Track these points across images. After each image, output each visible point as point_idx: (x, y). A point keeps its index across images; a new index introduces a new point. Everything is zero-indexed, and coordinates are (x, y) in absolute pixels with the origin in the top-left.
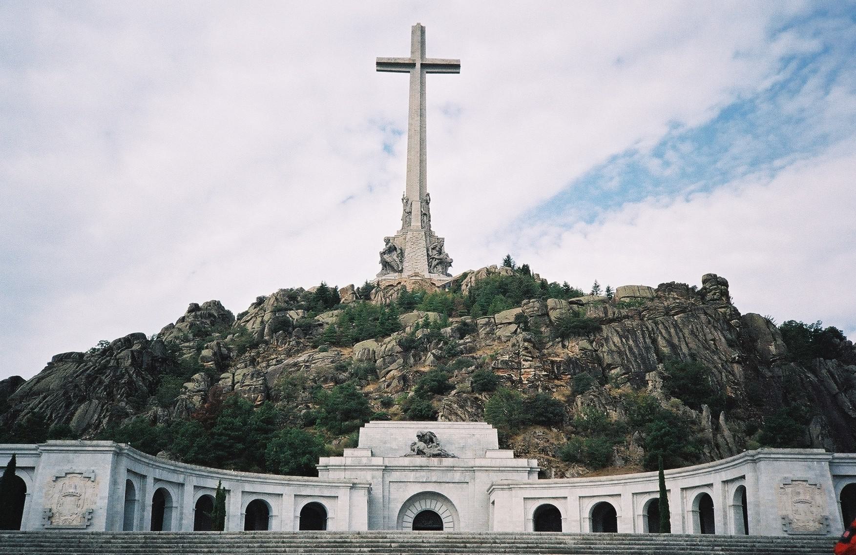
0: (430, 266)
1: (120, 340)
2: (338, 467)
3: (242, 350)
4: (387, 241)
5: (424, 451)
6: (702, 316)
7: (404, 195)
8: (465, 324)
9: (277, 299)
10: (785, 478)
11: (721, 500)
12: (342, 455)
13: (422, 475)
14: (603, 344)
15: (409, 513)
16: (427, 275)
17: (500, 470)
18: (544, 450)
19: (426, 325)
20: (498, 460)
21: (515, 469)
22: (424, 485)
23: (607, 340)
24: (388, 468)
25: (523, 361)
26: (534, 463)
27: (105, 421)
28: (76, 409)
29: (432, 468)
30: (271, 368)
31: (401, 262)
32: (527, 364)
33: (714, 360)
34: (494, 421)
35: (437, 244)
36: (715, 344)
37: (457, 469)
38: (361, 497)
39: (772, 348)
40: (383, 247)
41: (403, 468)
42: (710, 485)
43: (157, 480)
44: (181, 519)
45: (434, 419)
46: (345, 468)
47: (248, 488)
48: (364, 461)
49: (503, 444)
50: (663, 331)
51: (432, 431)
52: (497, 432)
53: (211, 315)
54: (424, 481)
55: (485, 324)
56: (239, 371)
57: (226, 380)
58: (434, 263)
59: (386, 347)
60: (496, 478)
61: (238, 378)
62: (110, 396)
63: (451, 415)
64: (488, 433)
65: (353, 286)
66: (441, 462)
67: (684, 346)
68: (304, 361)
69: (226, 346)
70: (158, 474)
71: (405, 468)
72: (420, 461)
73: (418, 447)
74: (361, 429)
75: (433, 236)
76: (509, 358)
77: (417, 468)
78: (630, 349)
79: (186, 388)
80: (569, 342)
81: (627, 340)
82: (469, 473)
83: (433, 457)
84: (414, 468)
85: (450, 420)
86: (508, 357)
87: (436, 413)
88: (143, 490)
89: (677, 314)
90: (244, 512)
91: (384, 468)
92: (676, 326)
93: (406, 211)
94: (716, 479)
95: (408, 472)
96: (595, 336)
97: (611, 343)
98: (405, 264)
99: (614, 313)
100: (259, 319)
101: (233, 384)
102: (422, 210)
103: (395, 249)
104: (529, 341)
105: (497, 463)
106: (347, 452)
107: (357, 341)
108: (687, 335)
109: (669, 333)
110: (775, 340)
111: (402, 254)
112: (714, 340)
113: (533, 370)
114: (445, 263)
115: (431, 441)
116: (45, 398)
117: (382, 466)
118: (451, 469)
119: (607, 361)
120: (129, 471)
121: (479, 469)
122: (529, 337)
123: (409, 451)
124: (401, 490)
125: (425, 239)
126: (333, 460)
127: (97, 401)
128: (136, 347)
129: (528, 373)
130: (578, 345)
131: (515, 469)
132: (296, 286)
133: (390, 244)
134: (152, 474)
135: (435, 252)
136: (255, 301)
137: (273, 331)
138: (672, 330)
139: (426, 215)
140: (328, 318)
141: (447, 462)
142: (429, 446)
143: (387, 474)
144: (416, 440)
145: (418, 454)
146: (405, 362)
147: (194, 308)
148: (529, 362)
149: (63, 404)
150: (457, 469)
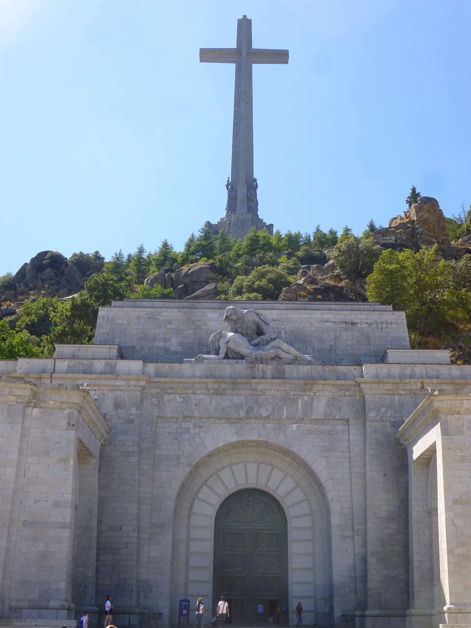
7: (228, 181)
73: (228, 342)
76: (396, 241)
91: (143, 383)
95: (202, 396)
102: (249, 195)
124: (187, 437)
145: (226, 357)
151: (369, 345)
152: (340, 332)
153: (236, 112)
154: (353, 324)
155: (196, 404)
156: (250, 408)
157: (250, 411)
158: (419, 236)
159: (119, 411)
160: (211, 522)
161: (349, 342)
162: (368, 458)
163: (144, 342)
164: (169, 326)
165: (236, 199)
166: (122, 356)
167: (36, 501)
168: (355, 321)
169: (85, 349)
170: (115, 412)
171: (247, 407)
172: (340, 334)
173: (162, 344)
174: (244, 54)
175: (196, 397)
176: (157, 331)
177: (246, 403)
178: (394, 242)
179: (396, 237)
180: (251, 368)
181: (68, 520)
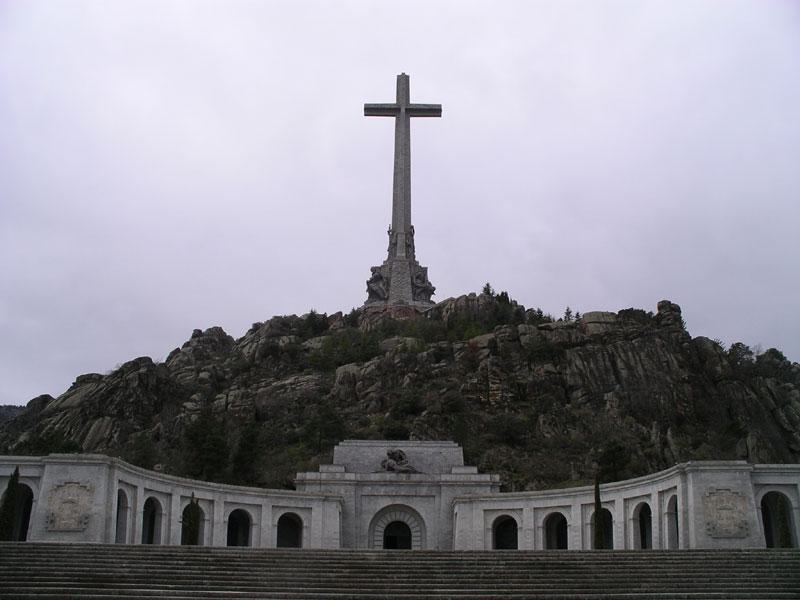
0: (414, 293)
1: (129, 363)
2: (313, 482)
3: (236, 373)
4: (374, 270)
6: (657, 340)
8: (441, 349)
9: (271, 326)
10: (711, 488)
11: (657, 509)
12: (318, 471)
13: (391, 490)
15: (380, 523)
16: (411, 303)
17: (464, 485)
18: (506, 467)
19: (405, 349)
21: (479, 484)
23: (570, 363)
26: (497, 477)
27: (116, 436)
28: (91, 425)
30: (260, 390)
31: (388, 290)
32: (495, 386)
33: (666, 381)
34: (460, 440)
36: (668, 365)
38: (333, 510)
39: (719, 369)
40: (369, 276)
42: (649, 496)
43: (146, 490)
44: (170, 525)
45: (405, 437)
46: (320, 483)
47: (230, 499)
48: (338, 476)
49: (468, 462)
50: (622, 355)
51: (402, 449)
53: (212, 341)
55: (460, 349)
56: (232, 393)
57: (221, 399)
58: (419, 290)
60: (459, 492)
61: (231, 398)
62: (121, 415)
63: (423, 435)
64: (453, 451)
65: (341, 313)
67: (640, 368)
68: (291, 384)
69: (222, 368)
70: (148, 484)
72: (389, 476)
74: (336, 448)
78: (591, 371)
79: (185, 407)
81: (588, 363)
85: (420, 439)
87: (407, 431)
88: (135, 498)
89: (634, 338)
90: (227, 519)
92: (633, 349)
94: (654, 490)
98: (391, 292)
99: (577, 338)
100: (255, 344)
101: (227, 404)
103: (381, 278)
104: (497, 365)
105: (463, 478)
106: (322, 468)
107: (340, 366)
108: (642, 358)
109: (627, 356)
110: (721, 361)
111: (388, 284)
112: (667, 362)
114: (430, 291)
115: (401, 458)
116: (66, 413)
118: (419, 484)
120: (120, 481)
122: (496, 361)
126: (310, 476)
127: (109, 418)
128: (142, 370)
129: (495, 395)
131: (479, 484)
132: (289, 313)
134: (142, 484)
135: (419, 281)
136: (251, 327)
137: (264, 356)
138: (630, 354)
140: (315, 343)
141: (415, 477)
146: (384, 385)
147: (197, 334)
149: (80, 420)
153: (396, 163)
160: (382, 534)
166: (346, 471)
174: (403, 110)
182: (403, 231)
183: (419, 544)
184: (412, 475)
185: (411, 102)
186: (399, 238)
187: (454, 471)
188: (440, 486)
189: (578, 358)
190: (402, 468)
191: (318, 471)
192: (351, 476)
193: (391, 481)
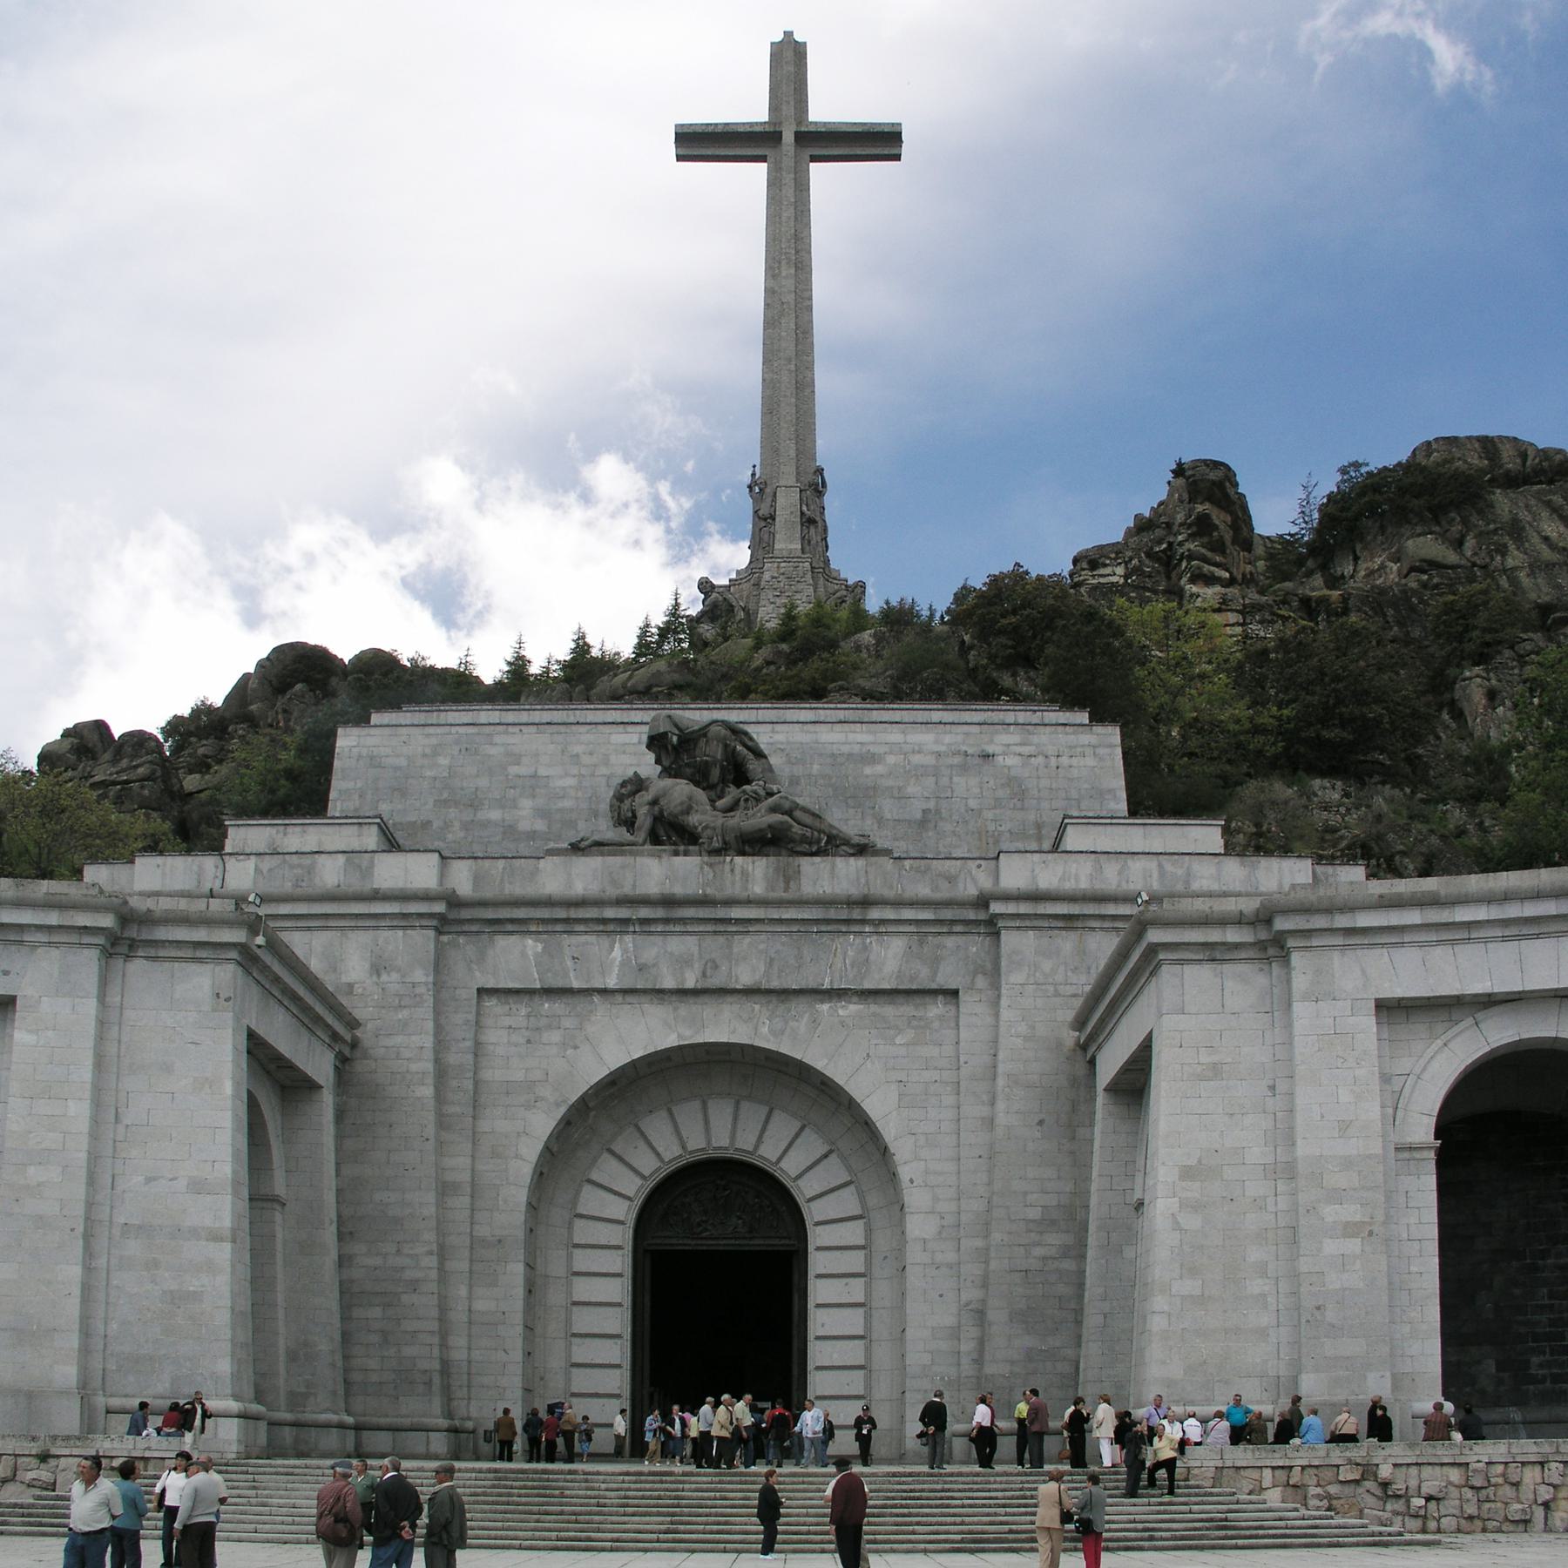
5: (694, 819)
7: (753, 475)
12: (216, 847)
14: (1505, 546)
20: (1137, 865)
22: (686, 1009)
23: (1516, 530)
24: (466, 914)
25: (1192, 581)
29: (737, 913)
32: (1211, 593)
35: (845, 593)
37: (889, 914)
41: (561, 913)
48: (330, 873)
52: (1118, 739)
54: (690, 983)
59: (630, 677)
66: (790, 877)
71: (574, 913)
73: (654, 802)
75: (835, 579)
76: (1126, 577)
77: (644, 912)
80: (1356, 559)
82: (961, 940)
83: (743, 853)
84: (623, 913)
86: (1120, 570)
91: (439, 908)
93: (760, 513)
95: (592, 938)
96: (1465, 522)
97: (1536, 540)
102: (804, 508)
113: (1232, 617)
115: (740, 776)
117: (426, 897)
119: (1533, 596)
121: (1024, 908)
123: (606, 829)
125: (811, 582)
130: (1396, 560)
133: (714, 595)
139: (812, 523)
142: (720, 803)
143: (463, 948)
144: (647, 765)
145: (655, 839)
148: (1218, 589)
150: (889, 914)
151: (1022, 809)
152: (951, 778)
154: (987, 756)
155: (574, 958)
156: (709, 964)
157: (709, 973)
158: (1184, 564)
159: (384, 977)
161: (973, 803)
162: (1001, 1082)
163: (453, 812)
164: (513, 770)
165: (774, 519)
166: (391, 843)
167: (149, 1180)
168: (990, 749)
169: (298, 829)
170: (375, 978)
171: (703, 962)
172: (951, 782)
173: (495, 815)
175: (575, 939)
176: (483, 782)
177: (700, 954)
178: (1122, 581)
179: (1127, 568)
180: (711, 865)
181: (227, 1222)
182: (792, 481)
183: (856, 1289)
184: (809, 866)
185: (811, 119)
186: (781, 501)
187: (1074, 839)
188: (992, 927)
189: (1545, 514)
190: (759, 818)
191: (216, 847)
192: (395, 872)
193: (668, 901)
